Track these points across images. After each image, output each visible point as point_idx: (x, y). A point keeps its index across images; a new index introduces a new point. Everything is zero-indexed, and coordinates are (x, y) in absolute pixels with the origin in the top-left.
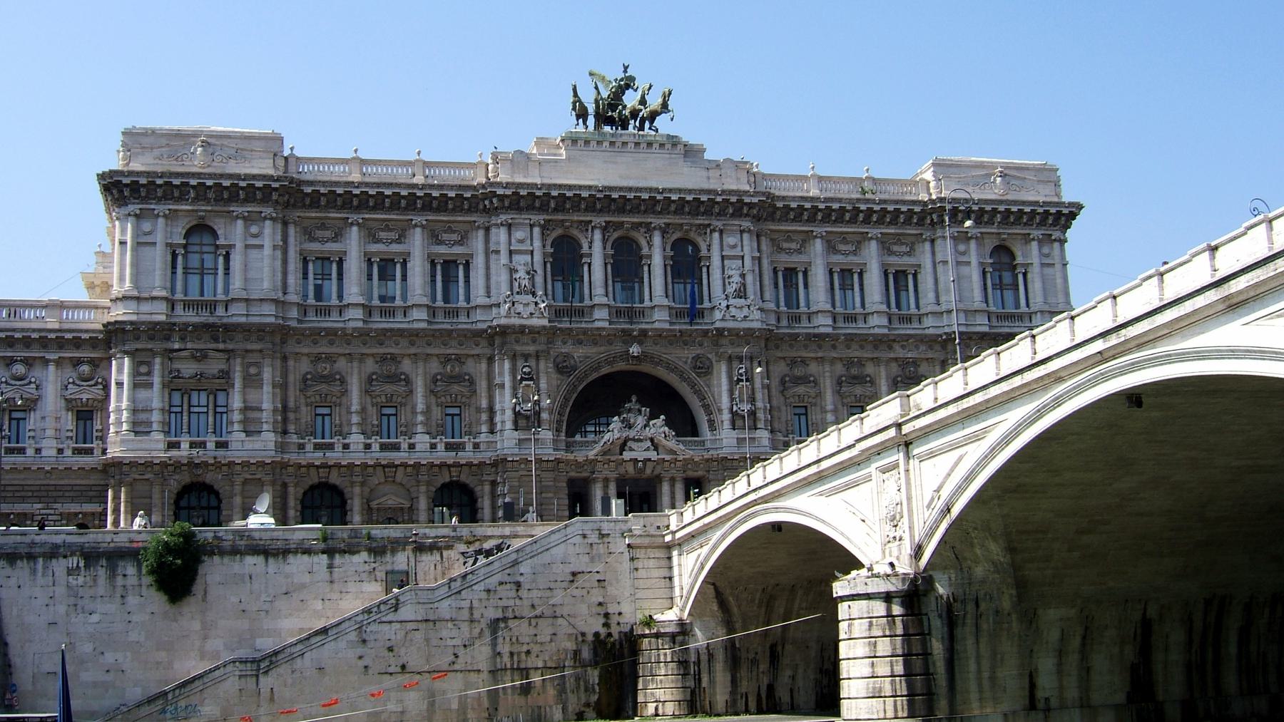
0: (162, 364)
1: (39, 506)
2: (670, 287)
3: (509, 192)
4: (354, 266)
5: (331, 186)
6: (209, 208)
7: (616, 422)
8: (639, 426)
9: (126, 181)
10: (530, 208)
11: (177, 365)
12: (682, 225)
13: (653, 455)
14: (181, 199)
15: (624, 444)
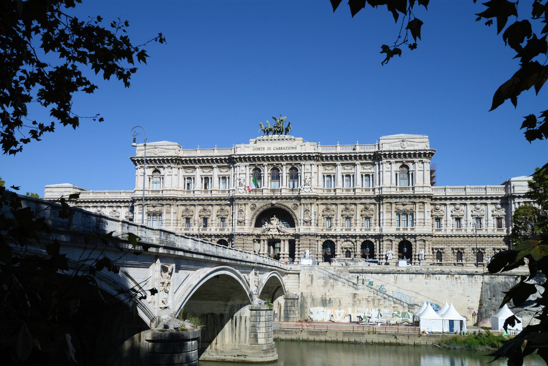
2: (288, 183)
3: (238, 157)
4: (198, 180)
6: (158, 165)
7: (266, 224)
10: (246, 161)
11: (149, 208)
12: (292, 163)
13: (277, 233)
15: (269, 229)
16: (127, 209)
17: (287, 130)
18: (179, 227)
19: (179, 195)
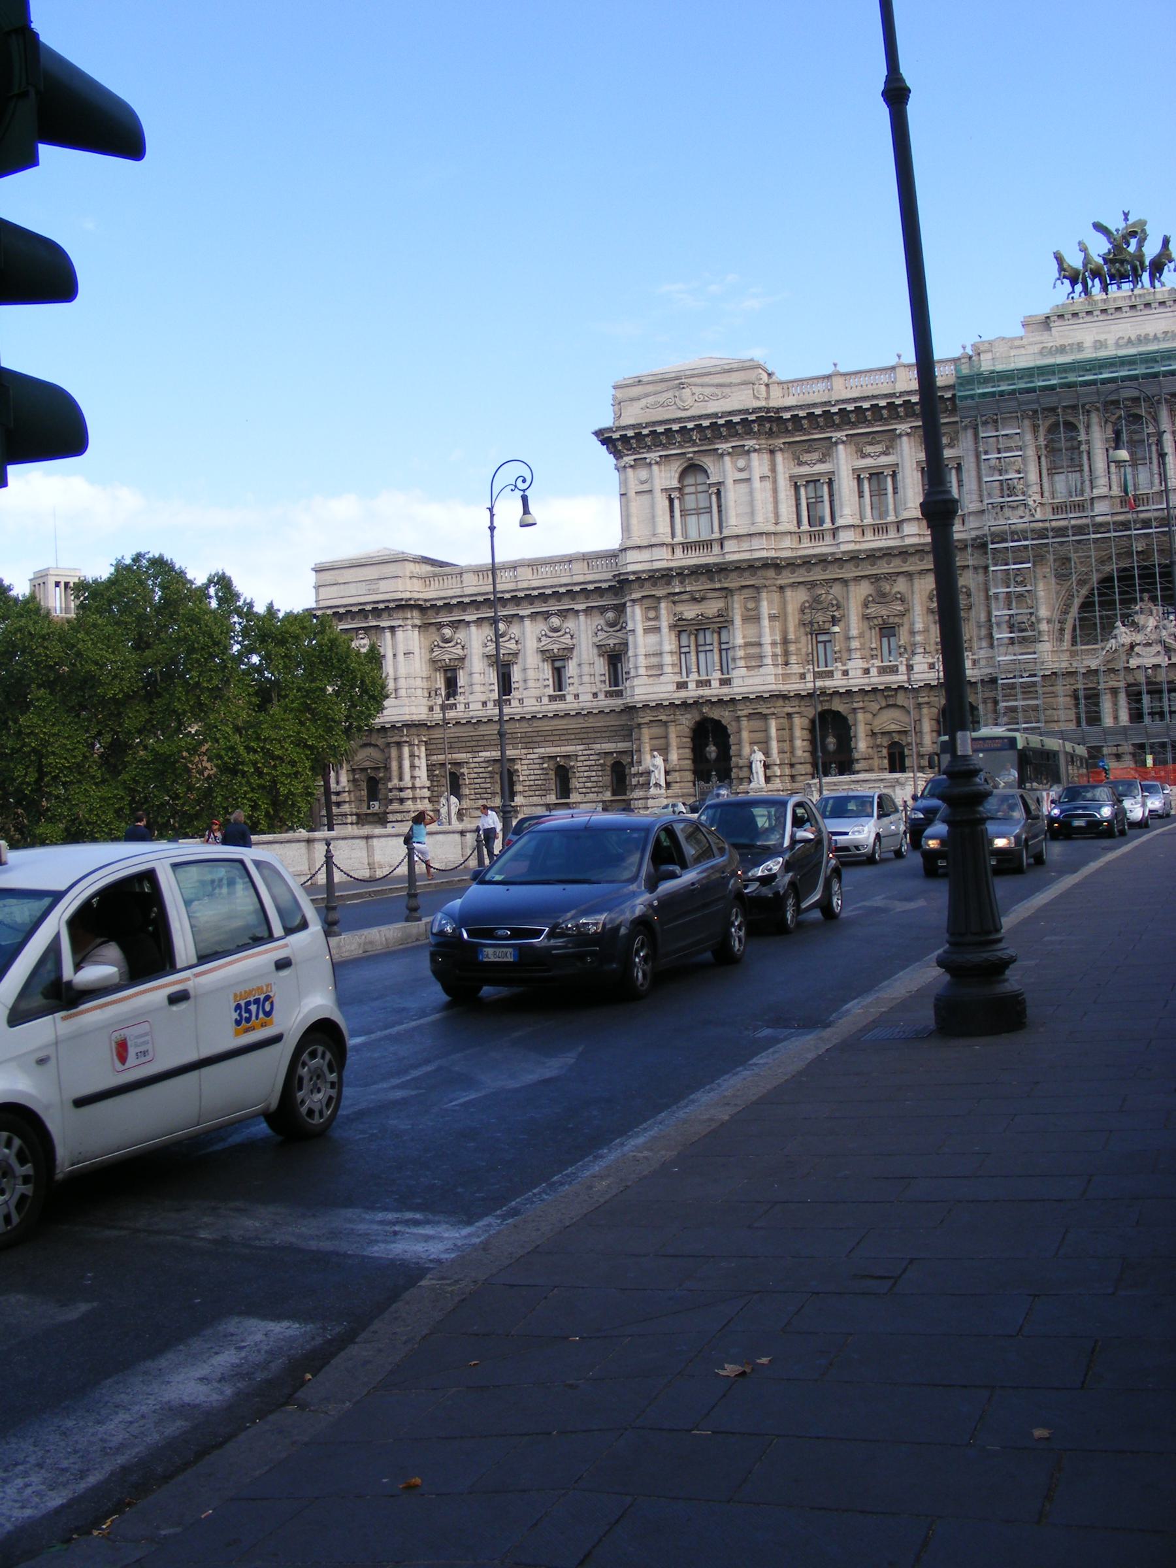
0: (667, 608)
1: (582, 747)
4: (846, 485)
5: (809, 408)
6: (696, 449)
8: (1149, 630)
9: (616, 436)
11: (680, 608)
13: (1163, 660)
14: (670, 443)
16: (598, 621)
17: (1157, 267)
18: (796, 669)
19: (786, 548)
